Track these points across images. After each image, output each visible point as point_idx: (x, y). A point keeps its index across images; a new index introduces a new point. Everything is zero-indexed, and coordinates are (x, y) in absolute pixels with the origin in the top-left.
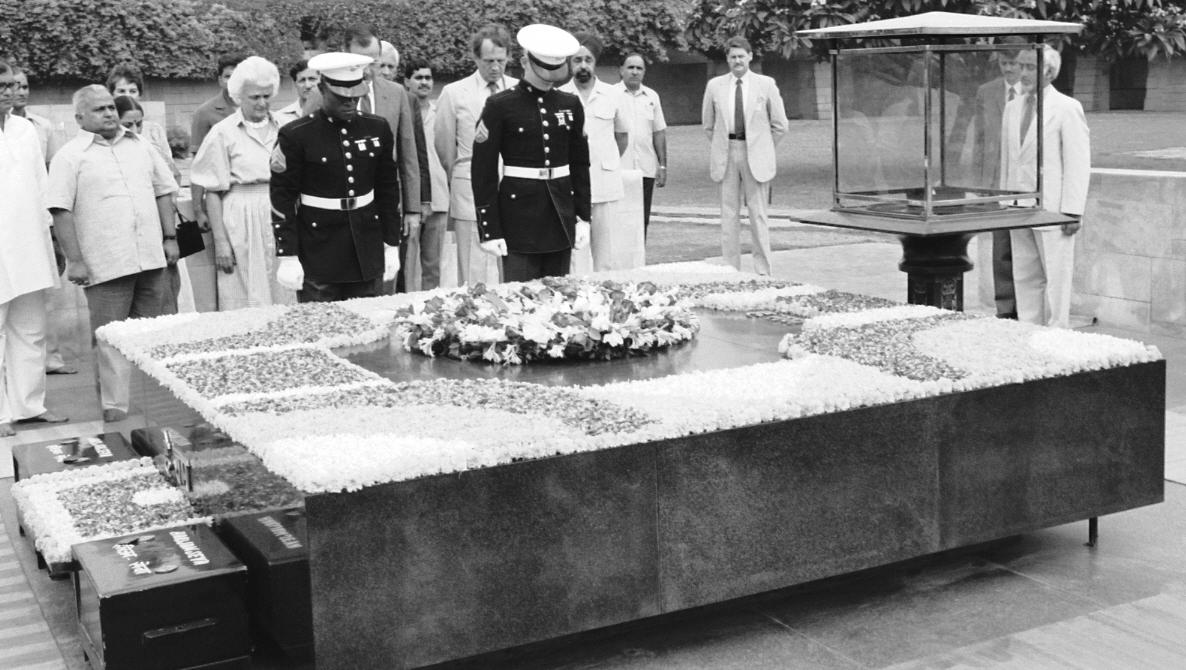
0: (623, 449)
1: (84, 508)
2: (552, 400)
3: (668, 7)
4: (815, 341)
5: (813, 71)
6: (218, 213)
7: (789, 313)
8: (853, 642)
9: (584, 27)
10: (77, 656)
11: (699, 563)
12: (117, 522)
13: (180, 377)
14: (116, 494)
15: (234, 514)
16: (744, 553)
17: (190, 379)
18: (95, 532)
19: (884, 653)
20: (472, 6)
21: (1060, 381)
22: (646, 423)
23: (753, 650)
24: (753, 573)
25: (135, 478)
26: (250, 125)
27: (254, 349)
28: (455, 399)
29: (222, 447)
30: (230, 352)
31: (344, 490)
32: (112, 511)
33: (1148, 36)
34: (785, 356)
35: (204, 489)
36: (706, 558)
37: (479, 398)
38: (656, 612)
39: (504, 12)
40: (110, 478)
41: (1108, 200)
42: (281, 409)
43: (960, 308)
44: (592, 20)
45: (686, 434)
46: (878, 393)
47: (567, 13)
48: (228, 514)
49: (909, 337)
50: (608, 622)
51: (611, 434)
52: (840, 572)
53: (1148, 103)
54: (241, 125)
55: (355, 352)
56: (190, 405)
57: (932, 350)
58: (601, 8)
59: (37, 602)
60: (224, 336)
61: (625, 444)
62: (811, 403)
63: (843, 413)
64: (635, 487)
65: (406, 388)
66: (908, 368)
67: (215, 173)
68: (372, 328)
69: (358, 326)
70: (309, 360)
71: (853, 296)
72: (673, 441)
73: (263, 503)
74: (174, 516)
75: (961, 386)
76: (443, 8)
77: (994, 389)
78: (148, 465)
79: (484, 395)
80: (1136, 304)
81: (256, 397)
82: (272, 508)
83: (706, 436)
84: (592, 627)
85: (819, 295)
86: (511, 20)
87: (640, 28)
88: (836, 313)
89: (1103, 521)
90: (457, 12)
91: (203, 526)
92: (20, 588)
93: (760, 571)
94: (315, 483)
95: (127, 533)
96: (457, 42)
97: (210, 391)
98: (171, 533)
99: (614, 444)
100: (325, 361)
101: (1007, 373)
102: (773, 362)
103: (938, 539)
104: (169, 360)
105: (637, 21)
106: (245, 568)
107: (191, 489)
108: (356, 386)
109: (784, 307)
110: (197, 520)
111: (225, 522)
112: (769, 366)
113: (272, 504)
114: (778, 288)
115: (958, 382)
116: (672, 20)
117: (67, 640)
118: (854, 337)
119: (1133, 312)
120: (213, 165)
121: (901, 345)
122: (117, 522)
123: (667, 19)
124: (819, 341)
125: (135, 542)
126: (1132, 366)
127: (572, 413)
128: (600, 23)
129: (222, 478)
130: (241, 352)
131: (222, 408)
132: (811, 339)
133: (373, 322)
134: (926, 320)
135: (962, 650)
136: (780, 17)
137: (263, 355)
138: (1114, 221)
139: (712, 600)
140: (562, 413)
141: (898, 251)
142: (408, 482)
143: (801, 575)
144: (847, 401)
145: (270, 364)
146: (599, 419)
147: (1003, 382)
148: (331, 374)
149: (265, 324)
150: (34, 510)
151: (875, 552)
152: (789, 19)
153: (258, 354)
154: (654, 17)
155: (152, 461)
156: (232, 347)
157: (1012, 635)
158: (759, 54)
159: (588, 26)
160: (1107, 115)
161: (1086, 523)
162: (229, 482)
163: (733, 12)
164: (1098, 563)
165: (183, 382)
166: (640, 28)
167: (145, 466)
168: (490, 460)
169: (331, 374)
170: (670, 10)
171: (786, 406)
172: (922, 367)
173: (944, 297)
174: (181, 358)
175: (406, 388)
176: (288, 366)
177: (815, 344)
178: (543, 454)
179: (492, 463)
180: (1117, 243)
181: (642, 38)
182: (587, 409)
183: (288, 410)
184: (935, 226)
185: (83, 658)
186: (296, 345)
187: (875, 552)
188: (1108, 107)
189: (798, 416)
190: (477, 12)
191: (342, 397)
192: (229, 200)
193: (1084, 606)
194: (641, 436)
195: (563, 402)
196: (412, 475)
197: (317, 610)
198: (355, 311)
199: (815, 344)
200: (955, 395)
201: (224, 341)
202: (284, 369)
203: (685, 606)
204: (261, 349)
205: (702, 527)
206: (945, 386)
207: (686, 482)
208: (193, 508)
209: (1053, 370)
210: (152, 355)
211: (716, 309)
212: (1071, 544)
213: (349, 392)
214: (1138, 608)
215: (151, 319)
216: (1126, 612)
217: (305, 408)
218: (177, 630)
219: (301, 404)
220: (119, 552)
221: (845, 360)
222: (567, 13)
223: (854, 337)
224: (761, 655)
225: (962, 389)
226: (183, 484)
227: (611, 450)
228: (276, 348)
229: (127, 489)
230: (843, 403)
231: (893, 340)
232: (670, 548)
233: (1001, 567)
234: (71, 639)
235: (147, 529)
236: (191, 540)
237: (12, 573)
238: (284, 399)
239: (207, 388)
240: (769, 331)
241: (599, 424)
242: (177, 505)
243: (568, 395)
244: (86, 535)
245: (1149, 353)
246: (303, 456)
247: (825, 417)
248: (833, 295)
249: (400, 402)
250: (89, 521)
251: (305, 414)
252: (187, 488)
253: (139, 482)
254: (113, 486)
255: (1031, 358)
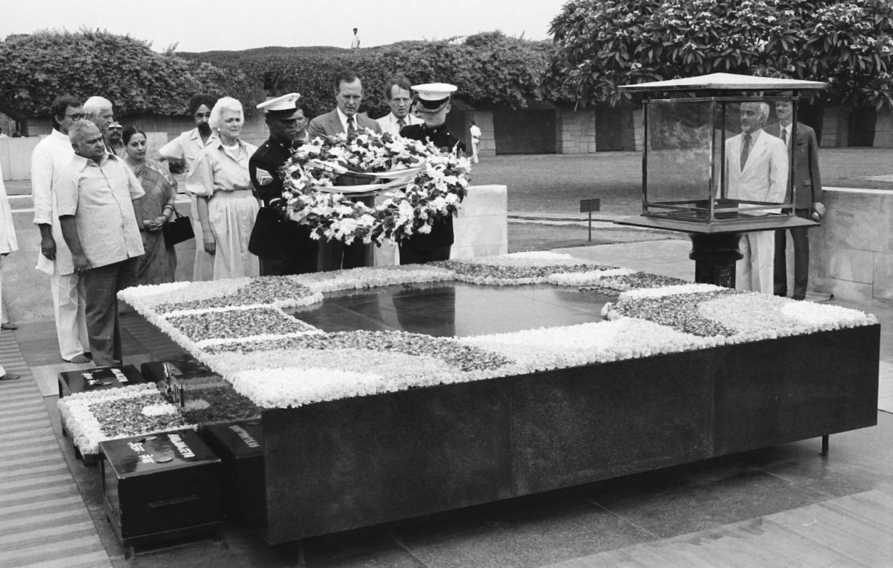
0: (487, 380)
1: (108, 417)
2: (438, 346)
3: (528, 69)
4: (628, 307)
5: (632, 116)
6: (205, 209)
7: (609, 288)
8: (651, 519)
9: (467, 82)
10: (102, 519)
11: (541, 462)
12: (131, 427)
13: (175, 327)
14: (130, 408)
15: (213, 423)
16: (573, 456)
17: (182, 328)
18: (116, 434)
19: (673, 528)
20: (386, 65)
21: (803, 337)
22: (505, 363)
23: (578, 524)
24: (580, 470)
25: (144, 397)
26: (226, 148)
27: (228, 308)
28: (369, 345)
29: (205, 376)
30: (210, 310)
31: (289, 407)
32: (128, 419)
33: (876, 93)
34: (606, 318)
35: (193, 405)
36: (546, 458)
37: (386, 345)
38: (510, 496)
39: (409, 70)
40: (126, 396)
41: (842, 209)
42: (246, 350)
43: (733, 286)
44: (473, 78)
45: (533, 371)
46: (672, 345)
47: (455, 72)
48: (207, 423)
49: (695, 306)
50: (475, 502)
51: (479, 371)
52: (642, 470)
53: (876, 142)
54: (220, 148)
55: (299, 311)
56: (182, 346)
57: (711, 315)
58: (480, 68)
59: (75, 482)
60: (207, 298)
61: (489, 378)
62: (623, 351)
63: (645, 359)
64: (495, 408)
65: (334, 337)
66: (693, 327)
67: (203, 183)
68: (312, 294)
69: (301, 292)
70: (266, 316)
71: (655, 277)
72: (524, 375)
73: (233, 416)
74: (171, 423)
75: (731, 340)
76: (365, 67)
77: (755, 343)
78: (153, 388)
79: (390, 342)
80: (861, 286)
81: (228, 341)
82: (238, 419)
83: (547, 373)
84: (464, 506)
85: (631, 275)
86: (415, 77)
87: (507, 84)
88: (643, 289)
89: (834, 439)
90: (376, 70)
91: (192, 430)
92: (63, 472)
93: (584, 469)
94: (269, 402)
95: (138, 435)
96: (376, 92)
97: (196, 337)
98: (169, 436)
99: (481, 378)
100: (278, 317)
101: (765, 332)
102: (597, 322)
103: (712, 448)
104: (168, 315)
105: (505, 78)
106: (220, 460)
107: (183, 405)
108: (299, 334)
109: (606, 283)
110: (186, 427)
111: (206, 428)
112: (594, 324)
113: (239, 417)
114: (602, 270)
115: (730, 338)
116: (531, 78)
117: (95, 508)
118: (655, 305)
119: (859, 291)
120: (201, 178)
121: (689, 312)
122: (131, 427)
123: (527, 77)
124: (631, 308)
125: (143, 441)
126: (855, 327)
127: (452, 355)
128: (478, 79)
129: (205, 398)
130: (219, 310)
131: (205, 348)
132: (625, 307)
133: (313, 290)
134: (708, 294)
135: (729, 527)
136: (609, 77)
137: (234, 312)
138: (847, 225)
139: (551, 488)
140: (445, 355)
141: (688, 245)
142: (334, 402)
143: (614, 471)
144: (649, 350)
145: (239, 319)
146: (471, 360)
147: (761, 338)
148: (282, 326)
149: (236, 290)
150: (73, 418)
151: (667, 457)
152: (614, 78)
153: (231, 311)
154: (518, 76)
155: (155, 385)
156: (213, 306)
157: (763, 517)
158: (594, 103)
159: (470, 82)
160: (847, 150)
161: (821, 438)
162: (209, 401)
163: (575, 73)
164: (828, 468)
165: (177, 330)
166: (507, 84)
167: (150, 389)
168: (393, 386)
169: (282, 326)
170: (530, 71)
171: (604, 353)
172: (704, 327)
173: (722, 278)
174: (177, 313)
175: (334, 337)
176: (252, 320)
177: (627, 310)
178: (431, 384)
179: (395, 390)
180: (849, 241)
181: (509, 91)
182: (462, 353)
183: (251, 350)
184: (716, 227)
185: (106, 521)
186: (257, 305)
187: (667, 457)
188: (846, 143)
189: (614, 360)
190: (390, 70)
191: (289, 342)
192: (213, 203)
193: (816, 497)
194: (501, 372)
195: (445, 348)
196: (337, 397)
197: (270, 490)
198: (300, 282)
199: (628, 310)
200: (727, 346)
201: (207, 302)
202: (249, 322)
203: (530, 493)
204: (233, 308)
205: (544, 437)
206: (720, 340)
207: (532, 405)
208: (184, 419)
209: (799, 330)
210: (156, 311)
211: (557, 285)
212: (809, 454)
213: (294, 339)
214: (855, 500)
215: (156, 286)
216: (846, 502)
217: (263, 350)
218: (172, 502)
219: (260, 347)
220: (132, 447)
221: (648, 322)
222: (455, 72)
223: (655, 305)
224: (584, 528)
225: (732, 343)
226: (177, 401)
227: (479, 382)
228: (244, 308)
229: (139, 404)
230: (646, 351)
231: (684, 308)
232: (520, 452)
233: (756, 469)
234: (99, 507)
235: (152, 432)
236: (182, 440)
237: (57, 462)
238: (248, 343)
239: (194, 335)
240: (592, 300)
241: (471, 363)
242: (173, 416)
243: (449, 343)
244: (109, 435)
245: (869, 319)
246: (261, 383)
247: (633, 360)
248: (641, 276)
249: (330, 346)
250: (112, 426)
251: (263, 354)
252: (180, 404)
253: (146, 400)
254: (128, 402)
255: (783, 321)
